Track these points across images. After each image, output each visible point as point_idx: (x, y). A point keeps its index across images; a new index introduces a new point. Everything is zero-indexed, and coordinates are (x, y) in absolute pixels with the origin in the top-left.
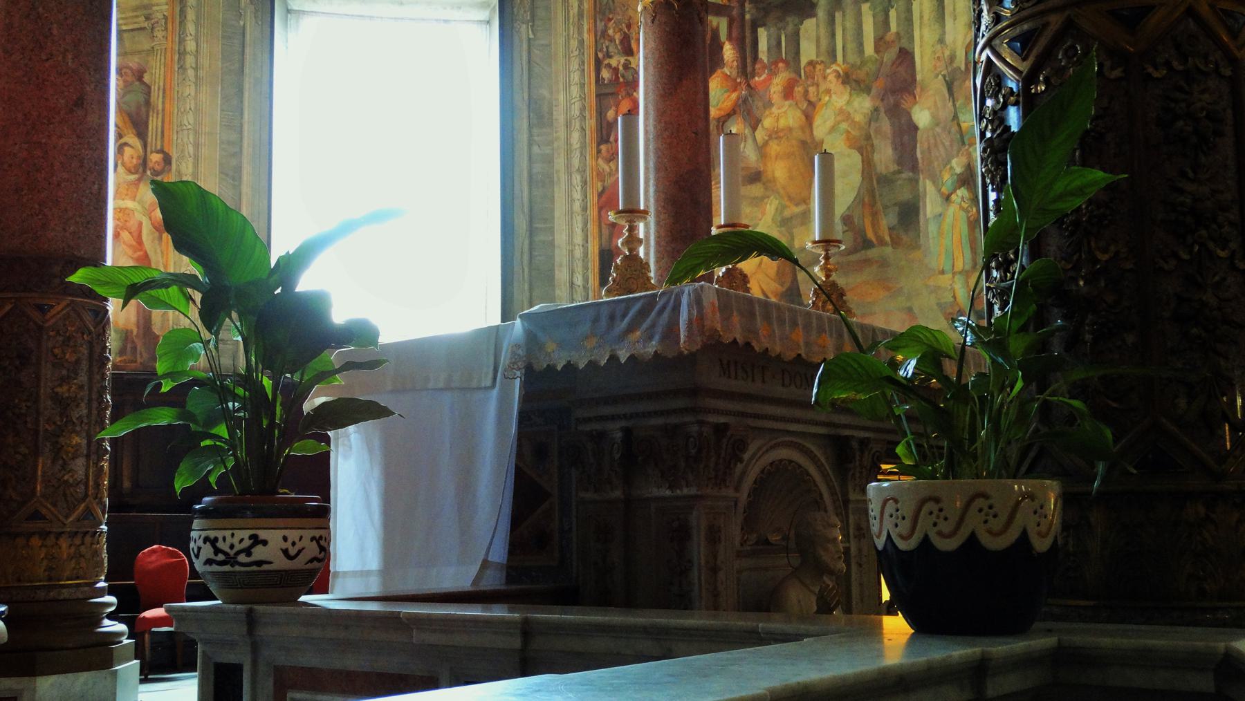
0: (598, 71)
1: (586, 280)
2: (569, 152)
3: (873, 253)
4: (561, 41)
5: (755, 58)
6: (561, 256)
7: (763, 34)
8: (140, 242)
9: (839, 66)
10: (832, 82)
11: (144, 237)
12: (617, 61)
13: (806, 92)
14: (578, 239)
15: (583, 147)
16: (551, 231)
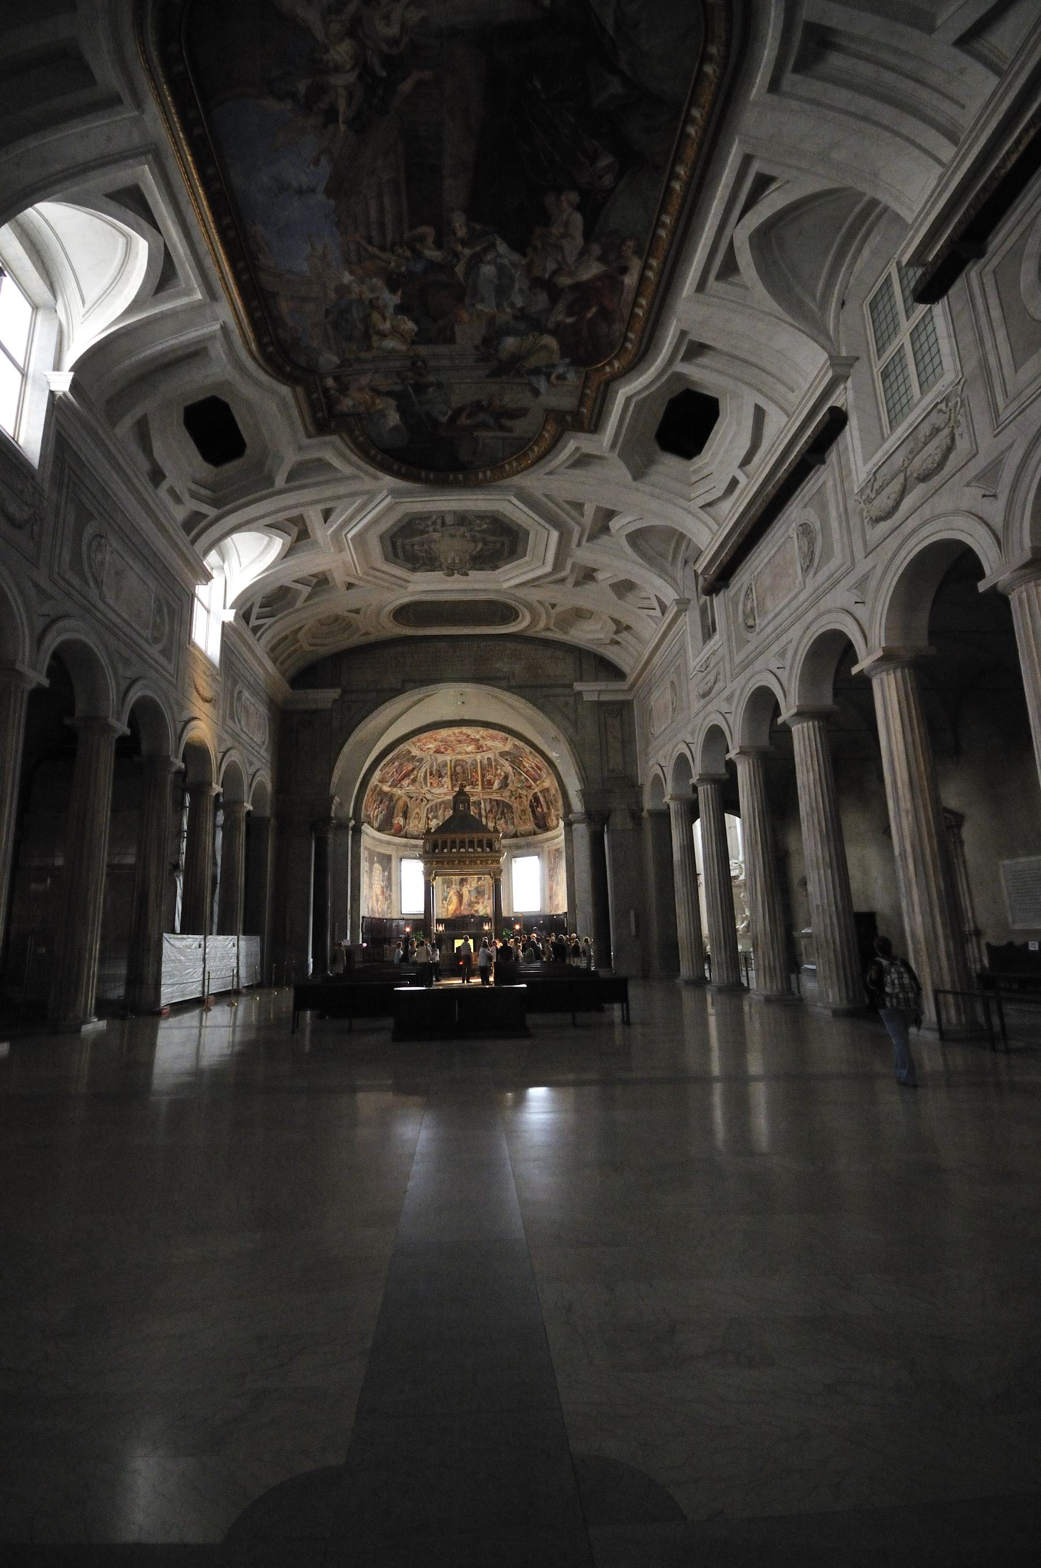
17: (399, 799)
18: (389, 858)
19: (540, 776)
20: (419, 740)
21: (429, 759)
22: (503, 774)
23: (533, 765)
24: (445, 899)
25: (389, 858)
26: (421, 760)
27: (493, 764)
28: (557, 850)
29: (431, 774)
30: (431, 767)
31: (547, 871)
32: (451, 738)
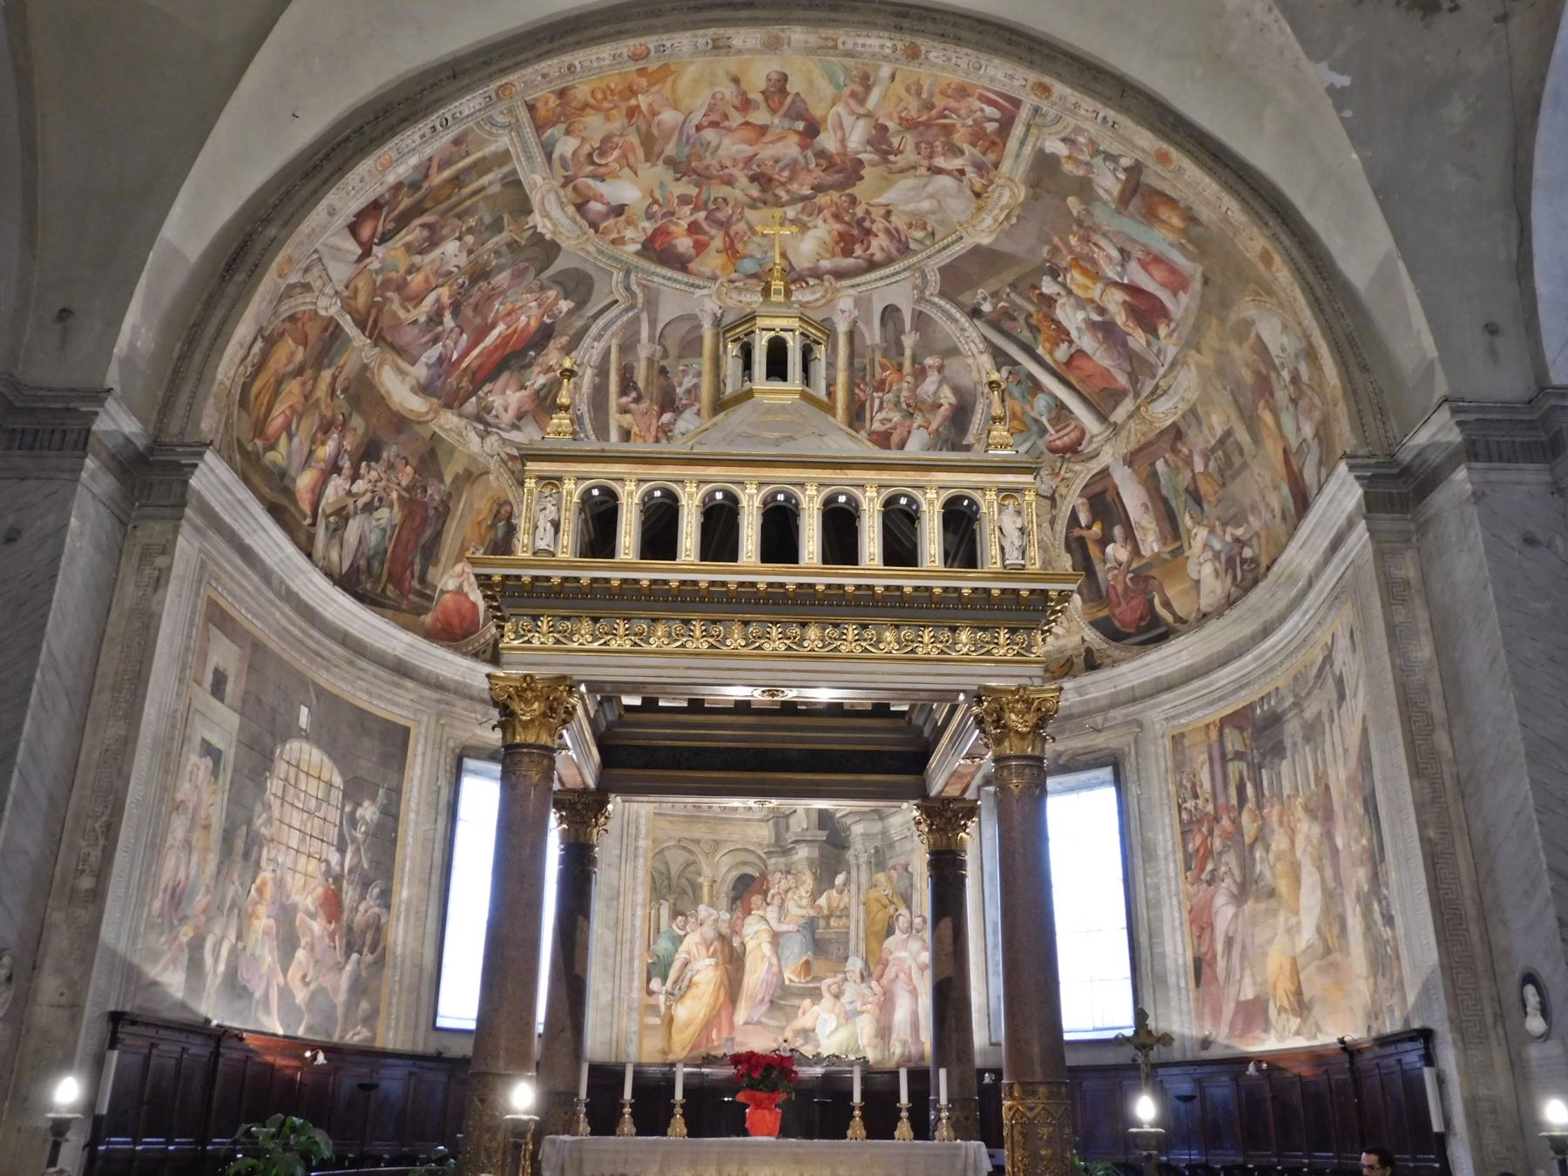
0: (1180, 814)
1: (1187, 983)
2: (1168, 879)
3: (1331, 958)
4: (1157, 794)
5: (1263, 794)
6: (1170, 965)
7: (1264, 771)
8: (911, 979)
9: (1300, 800)
10: (1300, 813)
11: (913, 972)
12: (1190, 804)
13: (1289, 821)
14: (1180, 950)
15: (1176, 875)
16: (1162, 944)
17: (470, 476)
18: (396, 740)
19: (1137, 366)
20: (567, 110)
21: (619, 294)
22: (948, 397)
23: (1115, 301)
24: (658, 968)
25: (396, 740)
26: (578, 286)
27: (909, 341)
28: (1236, 720)
29: (627, 385)
30: (628, 347)
31: (1165, 835)
32: (731, 147)
